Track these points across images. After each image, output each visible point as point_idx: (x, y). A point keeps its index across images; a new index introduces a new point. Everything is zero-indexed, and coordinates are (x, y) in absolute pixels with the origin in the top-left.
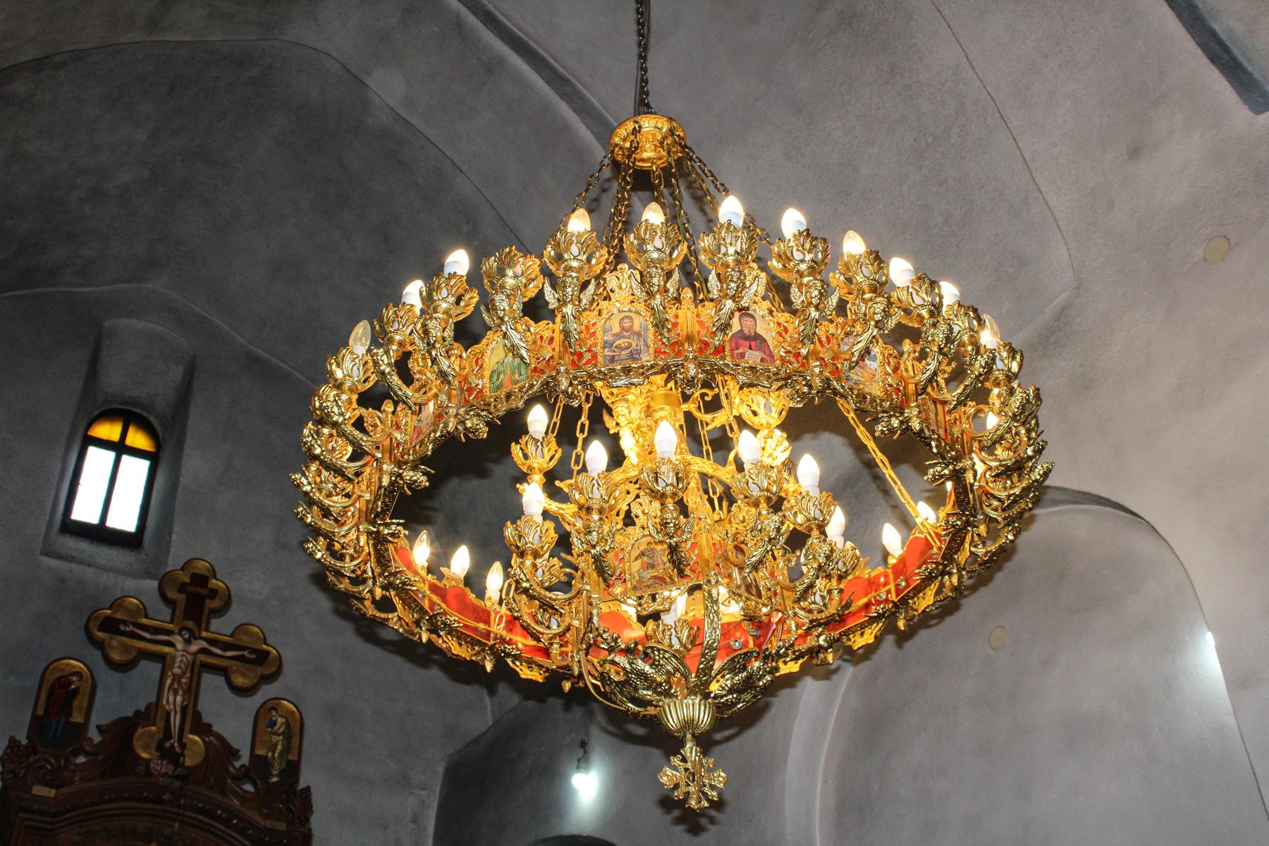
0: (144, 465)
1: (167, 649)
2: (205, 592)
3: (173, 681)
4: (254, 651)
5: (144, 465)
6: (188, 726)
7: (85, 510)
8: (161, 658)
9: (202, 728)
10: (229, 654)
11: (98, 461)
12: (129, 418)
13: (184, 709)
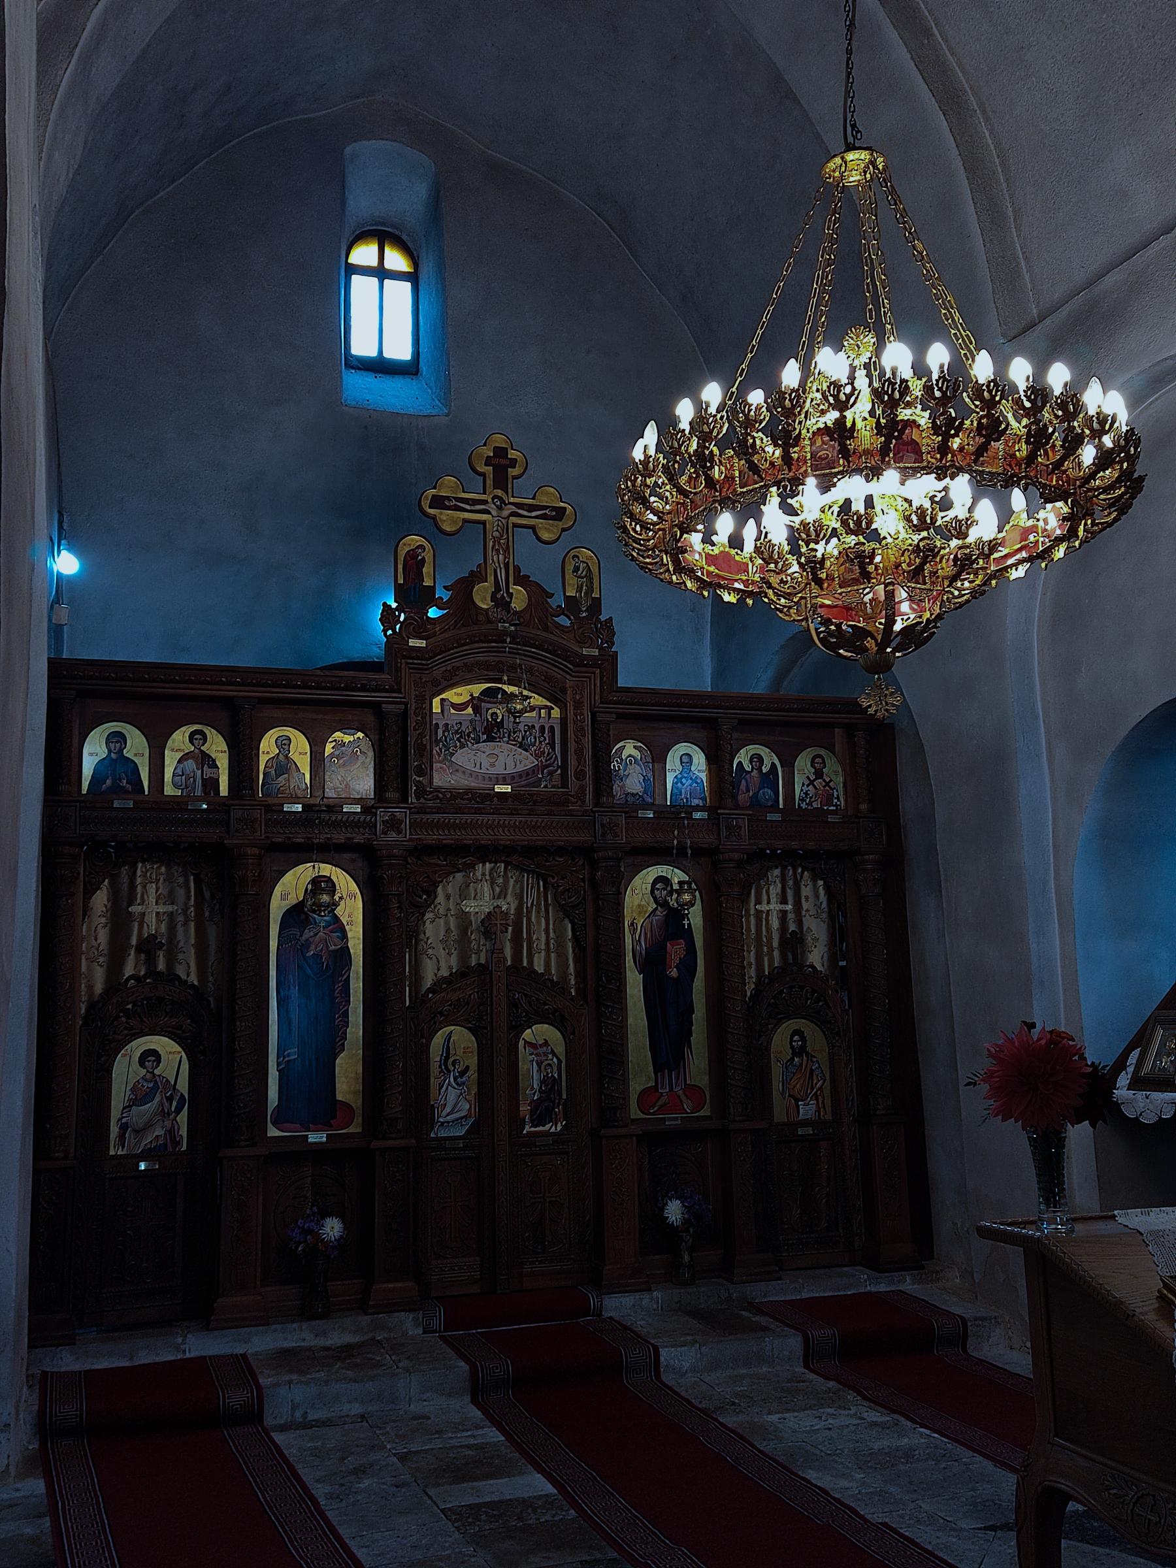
1: (484, 517)
3: (494, 542)
4: (554, 509)
6: (511, 579)
7: (362, 345)
8: (484, 523)
9: (523, 580)
10: (534, 514)
11: (362, 289)
12: (383, 237)
13: (507, 566)
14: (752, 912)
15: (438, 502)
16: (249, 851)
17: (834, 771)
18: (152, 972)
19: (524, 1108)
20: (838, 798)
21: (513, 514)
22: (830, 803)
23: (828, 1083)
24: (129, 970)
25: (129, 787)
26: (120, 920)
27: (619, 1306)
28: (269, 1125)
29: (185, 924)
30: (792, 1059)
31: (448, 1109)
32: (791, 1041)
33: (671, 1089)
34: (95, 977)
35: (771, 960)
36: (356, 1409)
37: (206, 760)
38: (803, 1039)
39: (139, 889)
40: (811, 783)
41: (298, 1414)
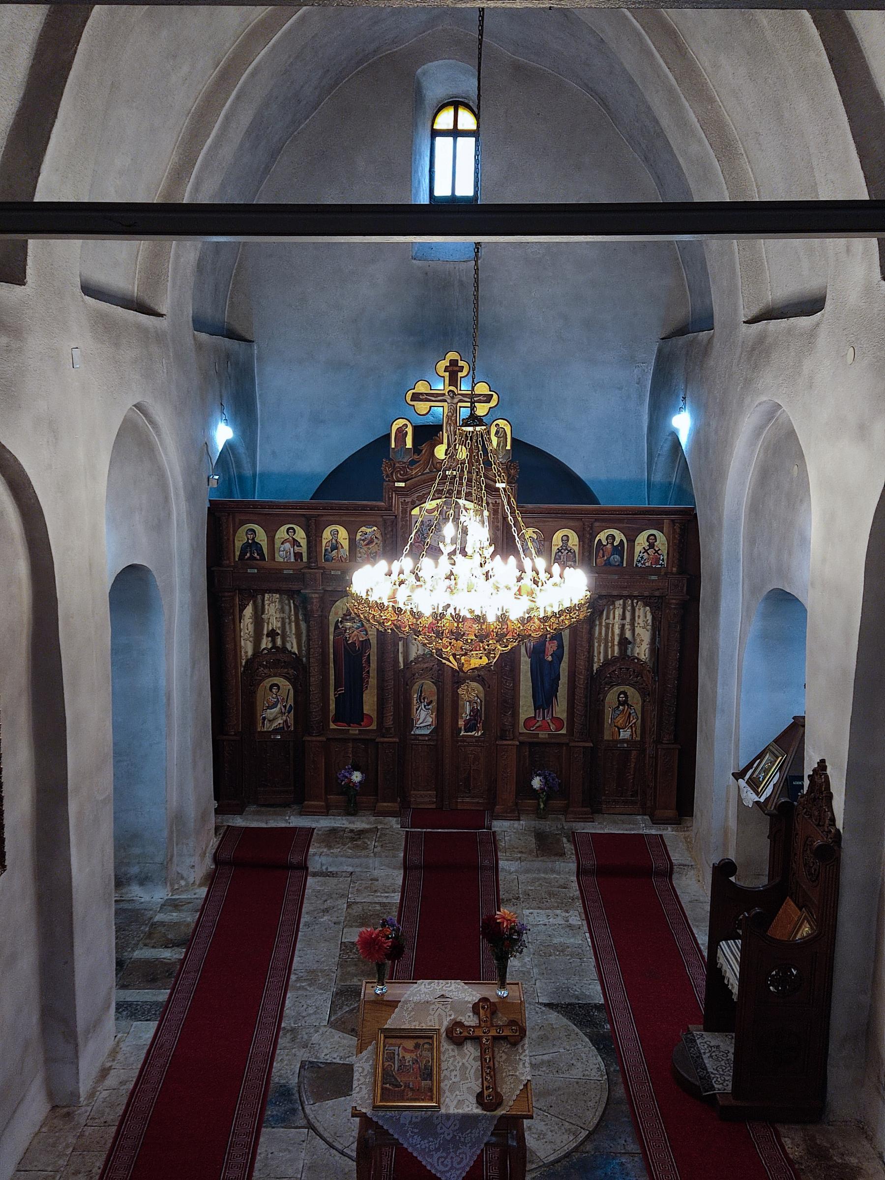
0: (472, 140)
2: (457, 369)
5: (472, 140)
11: (443, 144)
12: (456, 104)
14: (604, 624)
15: (416, 397)
16: (313, 596)
17: (662, 541)
18: (274, 646)
19: (461, 723)
20: (663, 560)
21: (461, 401)
22: (657, 563)
23: (639, 721)
24: (263, 646)
25: (258, 557)
26: (258, 621)
27: (499, 826)
28: (331, 723)
29: (290, 623)
30: (618, 707)
31: (420, 721)
32: (619, 697)
33: (544, 718)
34: (247, 648)
35: (613, 651)
36: (350, 869)
37: (295, 543)
38: (626, 696)
39: (266, 607)
40: (646, 551)
41: (324, 868)
